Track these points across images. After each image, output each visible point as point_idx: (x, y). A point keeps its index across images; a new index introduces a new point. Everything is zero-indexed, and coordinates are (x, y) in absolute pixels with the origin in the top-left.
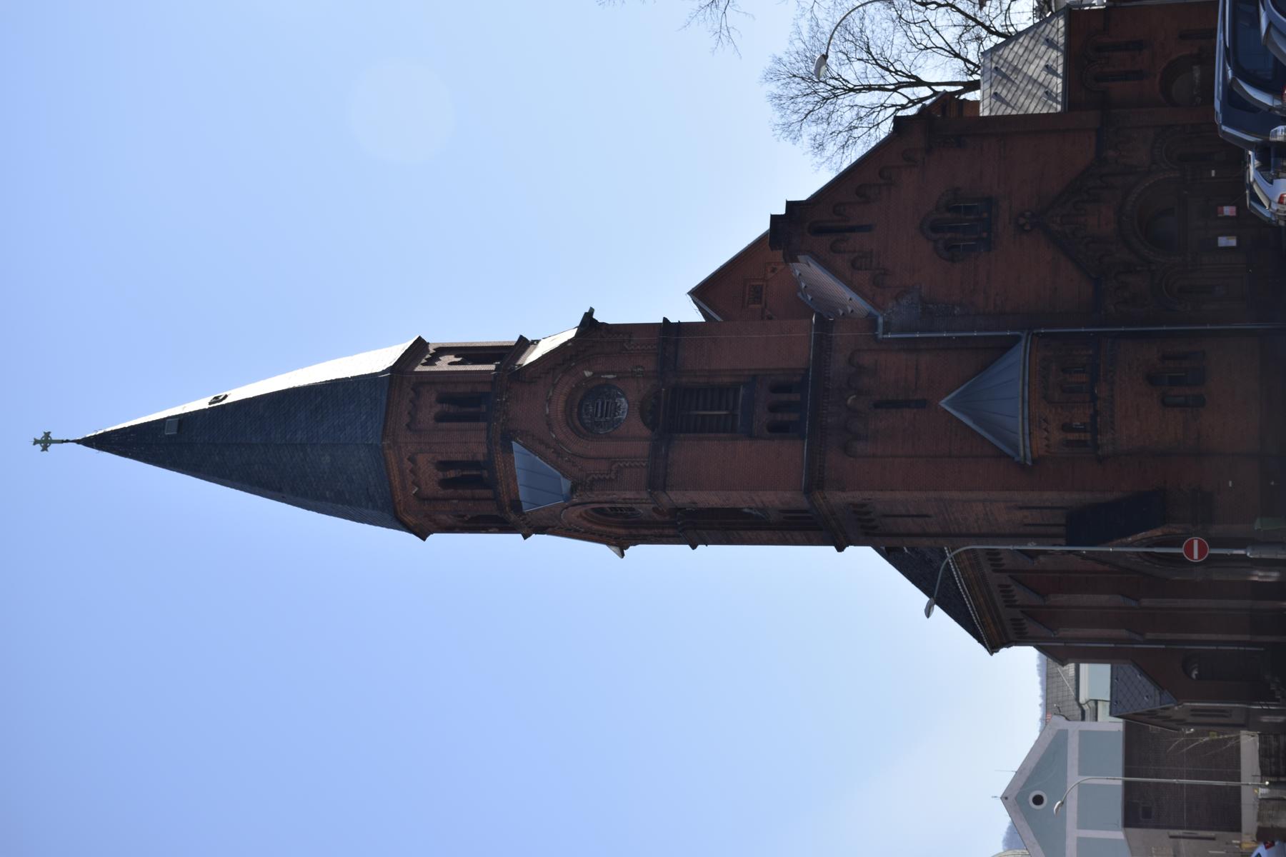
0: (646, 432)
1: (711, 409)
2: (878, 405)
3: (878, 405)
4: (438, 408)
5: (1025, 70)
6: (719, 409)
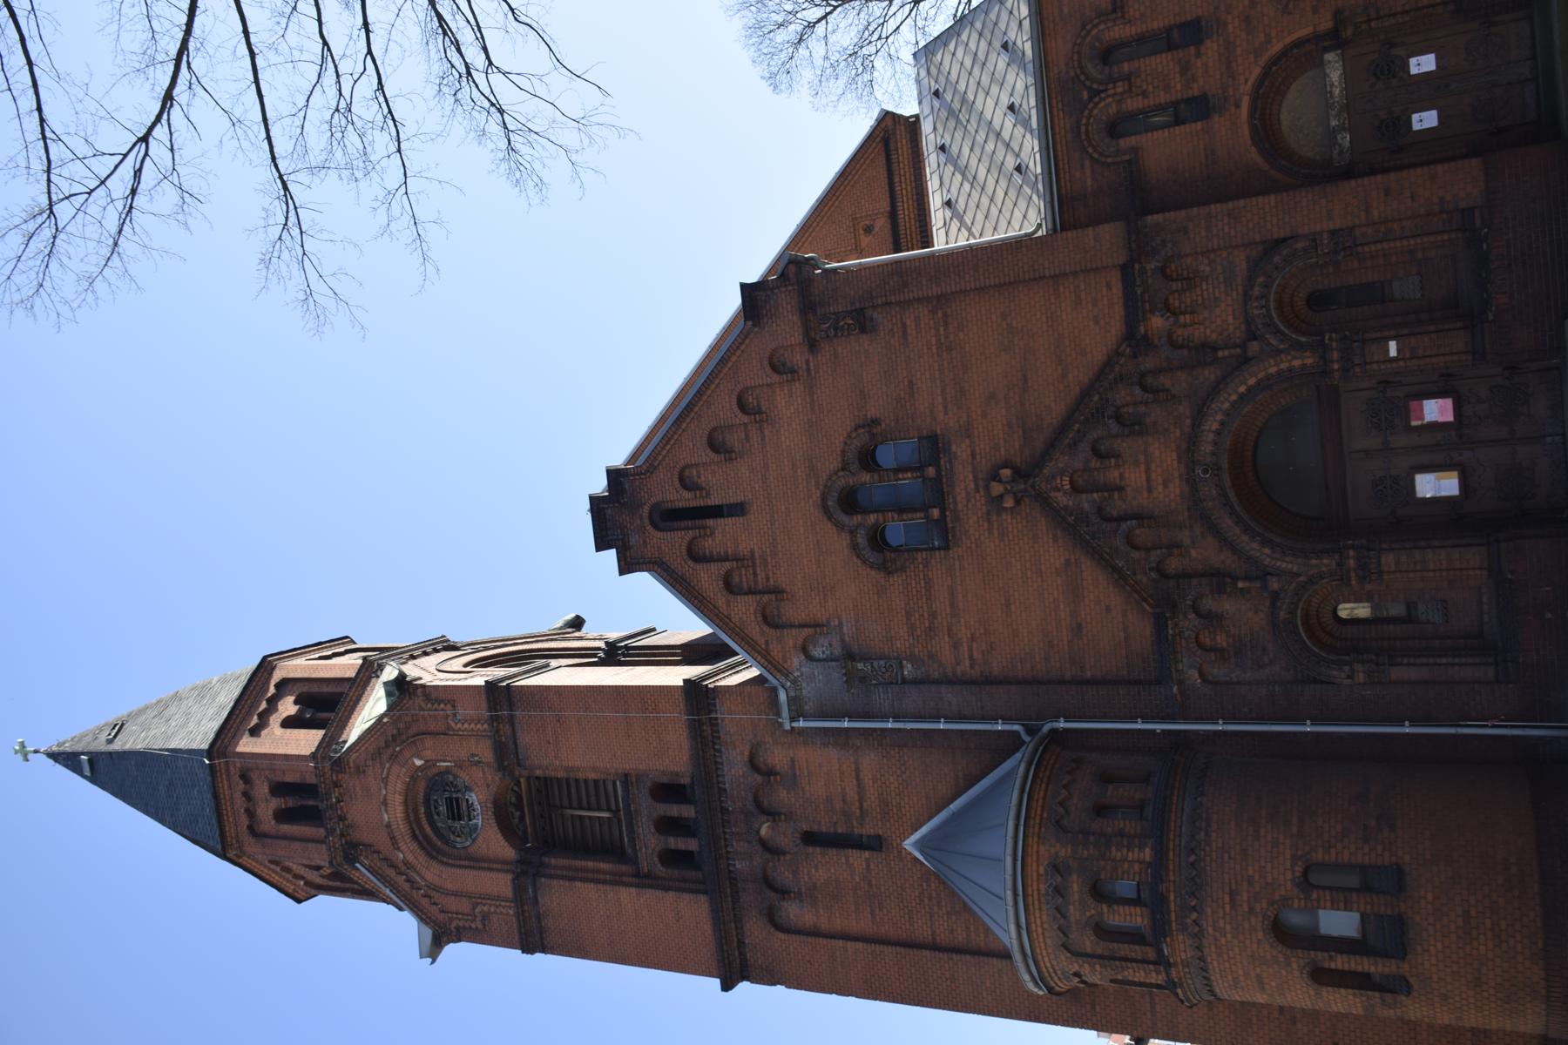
0: (509, 852)
1: (589, 809)
2: (810, 838)
3: (810, 838)
5: (979, 105)
6: (599, 809)
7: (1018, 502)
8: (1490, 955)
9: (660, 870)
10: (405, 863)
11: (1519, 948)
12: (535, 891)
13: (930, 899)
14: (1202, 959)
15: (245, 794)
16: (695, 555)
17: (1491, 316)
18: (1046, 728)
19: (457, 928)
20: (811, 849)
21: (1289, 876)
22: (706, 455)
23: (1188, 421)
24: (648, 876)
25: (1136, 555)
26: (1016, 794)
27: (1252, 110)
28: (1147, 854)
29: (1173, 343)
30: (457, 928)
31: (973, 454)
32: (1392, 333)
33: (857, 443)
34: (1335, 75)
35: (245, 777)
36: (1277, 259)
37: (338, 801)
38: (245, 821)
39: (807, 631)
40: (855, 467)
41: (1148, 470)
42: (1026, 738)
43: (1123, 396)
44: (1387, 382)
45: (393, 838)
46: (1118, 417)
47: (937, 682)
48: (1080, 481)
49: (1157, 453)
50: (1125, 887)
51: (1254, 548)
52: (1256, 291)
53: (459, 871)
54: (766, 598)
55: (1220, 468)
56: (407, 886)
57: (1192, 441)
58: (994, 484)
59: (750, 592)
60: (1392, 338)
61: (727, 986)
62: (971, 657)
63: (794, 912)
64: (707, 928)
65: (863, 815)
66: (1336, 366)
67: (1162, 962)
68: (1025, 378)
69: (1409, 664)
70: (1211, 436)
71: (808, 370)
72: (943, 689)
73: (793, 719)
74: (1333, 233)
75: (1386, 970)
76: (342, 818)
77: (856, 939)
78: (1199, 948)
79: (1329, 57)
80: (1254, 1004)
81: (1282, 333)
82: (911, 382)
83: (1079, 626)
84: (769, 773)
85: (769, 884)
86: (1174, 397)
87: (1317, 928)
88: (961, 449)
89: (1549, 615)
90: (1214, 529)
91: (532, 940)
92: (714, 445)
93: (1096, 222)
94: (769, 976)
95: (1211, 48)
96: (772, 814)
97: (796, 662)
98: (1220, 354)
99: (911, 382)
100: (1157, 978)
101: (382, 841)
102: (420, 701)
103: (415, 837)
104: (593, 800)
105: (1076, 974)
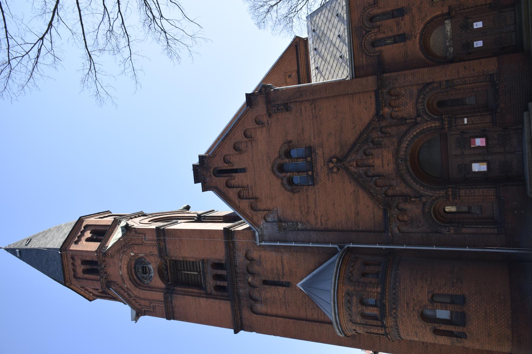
0: (162, 285)
1: (190, 271)
2: (265, 282)
3: (265, 282)
4: (83, 267)
5: (328, 35)
6: (194, 271)
7: (338, 170)
8: (493, 326)
9: (214, 292)
10: (127, 288)
11: (503, 323)
12: (171, 299)
13: (306, 303)
14: (397, 326)
15: (73, 264)
16: (228, 186)
17: (499, 111)
18: (346, 247)
19: (145, 311)
20: (265, 286)
21: (427, 298)
22: (233, 152)
23: (396, 144)
24: (210, 294)
25: (378, 189)
26: (335, 268)
27: (420, 39)
28: (379, 290)
29: (392, 117)
30: (145, 311)
31: (323, 153)
32: (466, 115)
33: (284, 149)
34: (448, 28)
35: (73, 258)
36: (427, 90)
37: (105, 267)
38: (72, 273)
39: (266, 212)
40: (283, 157)
41: (382, 160)
42: (339, 250)
43: (375, 135)
44: (464, 132)
45: (123, 280)
46: (373, 142)
47: (310, 230)
48: (359, 163)
49: (385, 154)
50: (372, 301)
51: (417, 187)
52: (420, 100)
53: (145, 291)
54: (252, 201)
55: (406, 160)
56: (127, 296)
57: (397, 151)
58: (330, 164)
59: (247, 198)
60: (465, 117)
61: (236, 332)
62: (321, 222)
63: (259, 307)
64: (230, 312)
65: (283, 275)
66: (446, 126)
67: (383, 326)
68: (342, 127)
69: (468, 227)
70: (404, 149)
71: (268, 124)
72: (312, 233)
73: (260, 242)
74: (447, 81)
75: (459, 330)
76: (106, 273)
77: (280, 317)
78: (396, 322)
79: (446, 22)
80: (414, 341)
81: (429, 115)
82: (303, 128)
83: (358, 212)
84: (252, 260)
85: (251, 297)
86: (392, 135)
87: (435, 316)
88: (319, 152)
89: (516, 212)
90: (404, 181)
91: (170, 316)
92: (236, 148)
93: (367, 76)
94: (250, 329)
95: (407, 17)
96: (253, 274)
97: (262, 222)
98: (408, 121)
99: (303, 128)
100: (382, 332)
101: (119, 281)
102: (133, 233)
103: (130, 280)
104: (192, 268)
105: (354, 330)
